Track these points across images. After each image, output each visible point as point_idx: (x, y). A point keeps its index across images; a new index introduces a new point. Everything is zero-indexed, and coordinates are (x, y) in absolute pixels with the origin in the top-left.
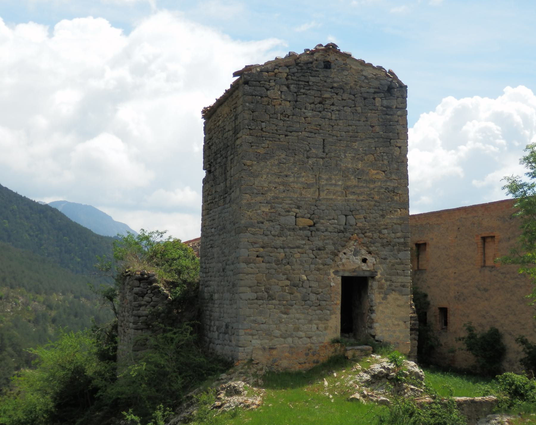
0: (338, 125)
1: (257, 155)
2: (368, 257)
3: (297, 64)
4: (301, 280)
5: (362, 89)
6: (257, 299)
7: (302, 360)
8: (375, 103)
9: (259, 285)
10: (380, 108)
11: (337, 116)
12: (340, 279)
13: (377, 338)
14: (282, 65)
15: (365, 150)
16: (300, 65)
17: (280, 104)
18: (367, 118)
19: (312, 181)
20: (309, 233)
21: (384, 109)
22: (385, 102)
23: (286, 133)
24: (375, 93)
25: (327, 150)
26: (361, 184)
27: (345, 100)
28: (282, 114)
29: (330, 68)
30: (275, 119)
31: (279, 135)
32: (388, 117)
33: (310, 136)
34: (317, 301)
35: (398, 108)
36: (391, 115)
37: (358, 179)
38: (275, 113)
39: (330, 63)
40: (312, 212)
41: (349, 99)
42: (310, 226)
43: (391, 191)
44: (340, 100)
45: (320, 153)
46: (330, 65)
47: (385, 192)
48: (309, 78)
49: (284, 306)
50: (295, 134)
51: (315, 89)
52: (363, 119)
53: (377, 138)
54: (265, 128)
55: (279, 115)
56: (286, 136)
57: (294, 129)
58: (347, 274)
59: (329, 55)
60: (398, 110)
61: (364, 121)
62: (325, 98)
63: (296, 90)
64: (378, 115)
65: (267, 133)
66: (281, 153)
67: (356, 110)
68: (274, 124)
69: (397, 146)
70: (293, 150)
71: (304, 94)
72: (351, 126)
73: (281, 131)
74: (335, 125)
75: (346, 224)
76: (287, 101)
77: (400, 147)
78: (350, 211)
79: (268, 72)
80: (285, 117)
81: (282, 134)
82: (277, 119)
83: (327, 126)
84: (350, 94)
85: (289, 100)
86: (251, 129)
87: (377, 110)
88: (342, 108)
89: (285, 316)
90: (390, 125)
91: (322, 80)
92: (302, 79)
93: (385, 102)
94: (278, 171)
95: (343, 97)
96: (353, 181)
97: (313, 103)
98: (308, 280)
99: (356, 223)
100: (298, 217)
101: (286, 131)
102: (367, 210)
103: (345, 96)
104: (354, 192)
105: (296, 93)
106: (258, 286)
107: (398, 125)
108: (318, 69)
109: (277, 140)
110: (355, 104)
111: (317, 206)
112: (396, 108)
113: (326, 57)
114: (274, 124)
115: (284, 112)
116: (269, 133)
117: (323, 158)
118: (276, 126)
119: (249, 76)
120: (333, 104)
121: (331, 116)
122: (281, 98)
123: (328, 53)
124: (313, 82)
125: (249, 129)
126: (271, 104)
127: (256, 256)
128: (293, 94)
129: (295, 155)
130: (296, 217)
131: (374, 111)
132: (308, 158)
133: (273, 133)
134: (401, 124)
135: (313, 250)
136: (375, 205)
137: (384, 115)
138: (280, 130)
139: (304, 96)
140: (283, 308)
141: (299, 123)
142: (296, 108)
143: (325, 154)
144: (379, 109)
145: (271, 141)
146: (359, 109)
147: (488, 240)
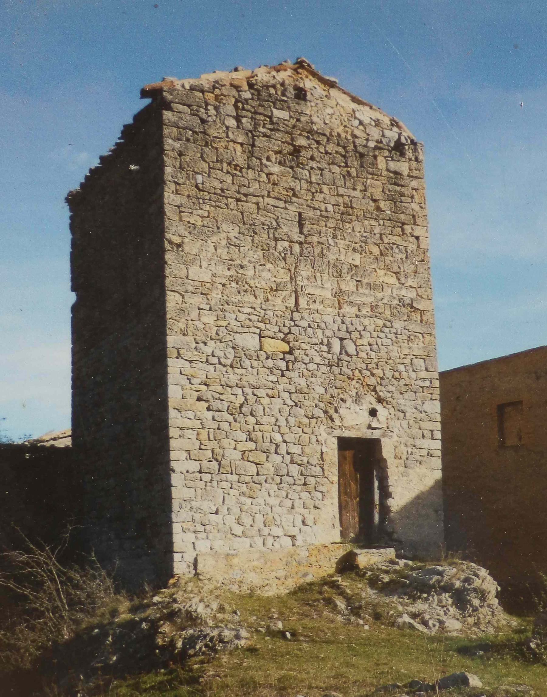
0: (321, 192)
1: (189, 227)
2: (379, 407)
3: (398, 672)
4: (273, 441)
5: (357, 139)
6: (200, 472)
7: (281, 573)
8: (377, 164)
9: (203, 447)
10: (385, 173)
11: (319, 177)
12: (336, 441)
13: (395, 536)
14: (225, 83)
15: (365, 237)
16: (256, 87)
17: (226, 148)
18: (365, 186)
19: (283, 277)
20: (282, 365)
21: (392, 175)
22: (393, 165)
23: (238, 196)
24: (376, 148)
25: (305, 231)
26: (361, 291)
27: (330, 154)
28: (229, 164)
29: (305, 100)
30: (218, 171)
31: (227, 198)
32: (398, 188)
33: (277, 205)
34: (300, 477)
35: (412, 177)
36: (402, 186)
37: (357, 281)
38: (217, 161)
39: (306, 91)
40: (286, 330)
41: (337, 152)
42: (285, 353)
43: (408, 304)
44: (322, 153)
45: (296, 236)
46: (305, 95)
47: (399, 305)
48: (272, 112)
49: (246, 483)
50: (254, 200)
51: (282, 129)
52: (359, 187)
53: (383, 219)
54: (203, 184)
55: (225, 165)
56: (238, 200)
57: (251, 190)
58: (347, 434)
59: (301, 78)
60: (411, 179)
61: (361, 191)
62: (299, 146)
63: (250, 127)
64: (383, 184)
65: (206, 193)
66: (231, 228)
67: (348, 172)
68: (217, 179)
69: (412, 236)
70: (251, 225)
71: (264, 136)
72: (342, 196)
73: (229, 192)
74: (317, 191)
75: (341, 354)
76: (238, 143)
77: (417, 238)
78: (347, 332)
79: (203, 91)
80: (235, 169)
81: (231, 197)
82: (222, 171)
83: (303, 192)
84: (338, 145)
85: (240, 141)
86: (179, 184)
87: (381, 175)
88: (327, 166)
89: (249, 501)
90: (401, 202)
91: (293, 118)
92: (261, 110)
93: (393, 165)
94: (227, 258)
95: (327, 149)
96: (349, 285)
97: (280, 152)
98: (284, 441)
99: (358, 353)
100: (264, 337)
101: (239, 193)
102: (373, 332)
103: (331, 148)
104: (352, 302)
105: (251, 131)
106: (200, 449)
107: (412, 202)
108: (285, 98)
109: (223, 205)
110: (346, 163)
111: (294, 321)
112: (409, 176)
113: (297, 80)
114: (217, 179)
115: (233, 160)
116: (209, 193)
117: (301, 243)
118: (221, 182)
119: (171, 94)
120: (312, 158)
121: (310, 177)
122: (227, 137)
123: (300, 76)
124: (279, 118)
125: (175, 182)
126: (211, 145)
127: (196, 398)
128: (247, 134)
129: (255, 233)
130: (260, 336)
131: (375, 177)
132: (276, 239)
133: (215, 194)
134: (417, 202)
135: (290, 393)
136: (385, 326)
137: (391, 184)
138: (227, 190)
139: (264, 139)
140: (244, 488)
141: (259, 182)
142: (252, 156)
143: (303, 237)
144: (383, 174)
145: (213, 206)
146: (353, 172)
147: (508, 409)
